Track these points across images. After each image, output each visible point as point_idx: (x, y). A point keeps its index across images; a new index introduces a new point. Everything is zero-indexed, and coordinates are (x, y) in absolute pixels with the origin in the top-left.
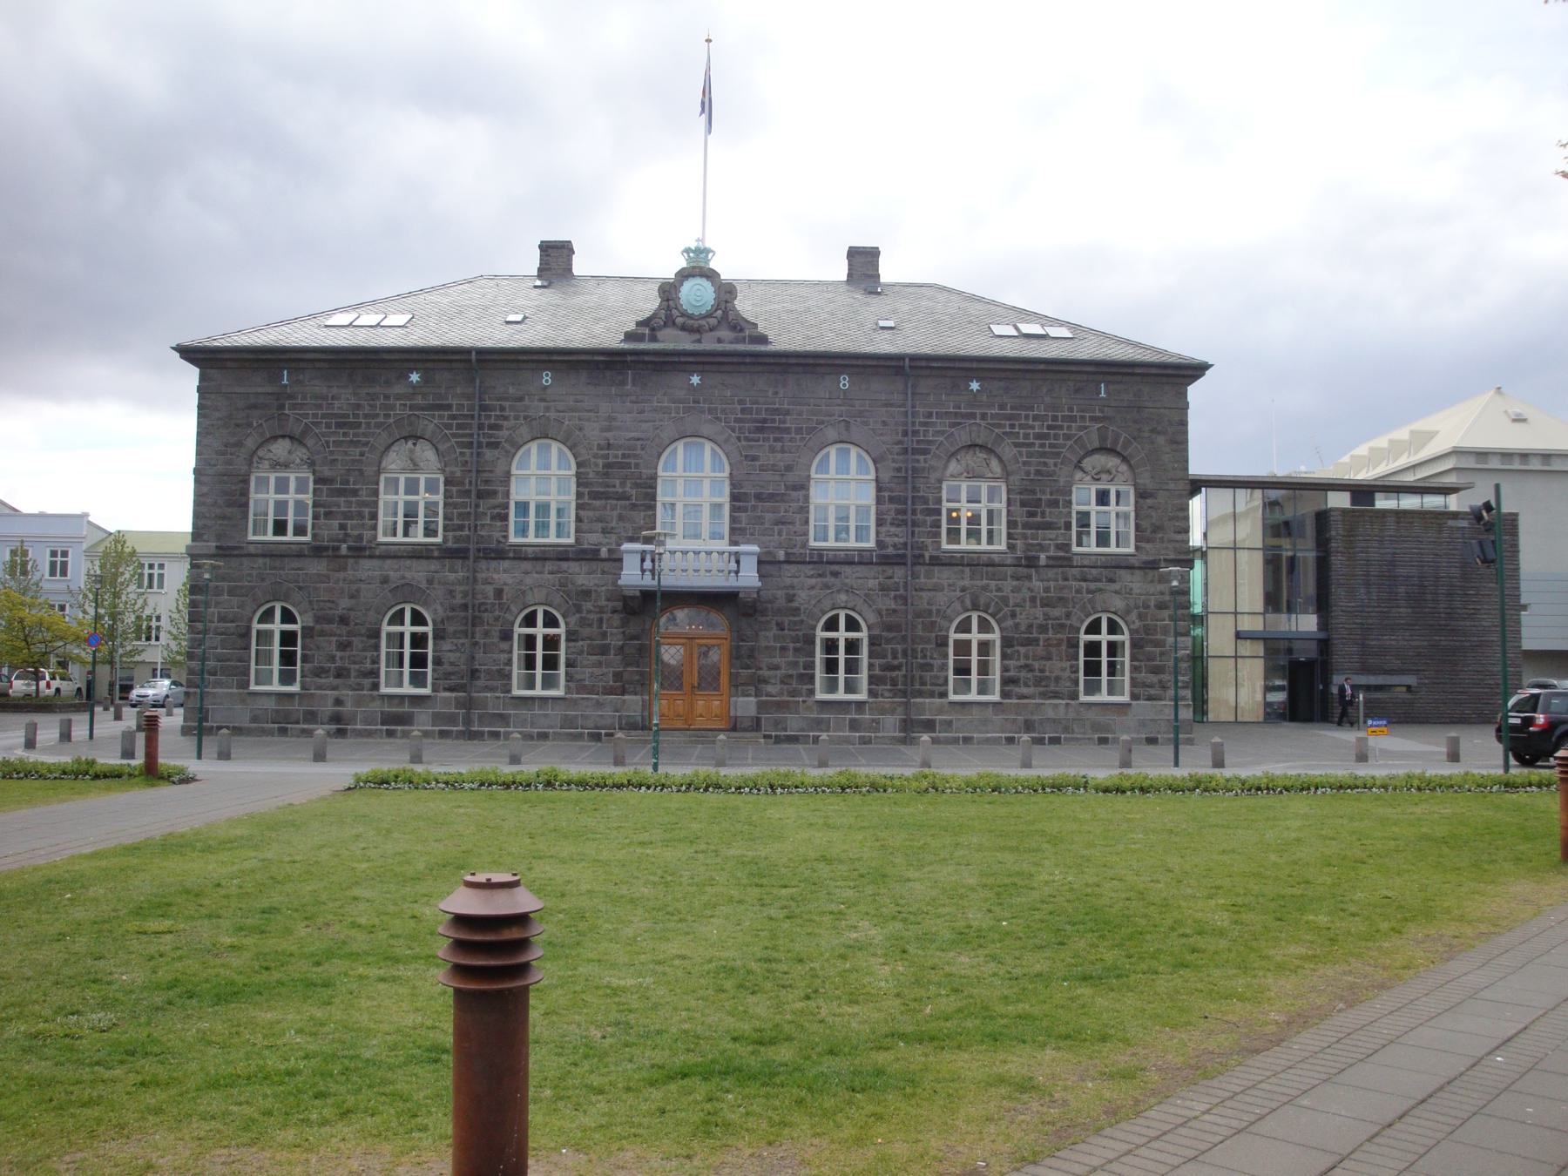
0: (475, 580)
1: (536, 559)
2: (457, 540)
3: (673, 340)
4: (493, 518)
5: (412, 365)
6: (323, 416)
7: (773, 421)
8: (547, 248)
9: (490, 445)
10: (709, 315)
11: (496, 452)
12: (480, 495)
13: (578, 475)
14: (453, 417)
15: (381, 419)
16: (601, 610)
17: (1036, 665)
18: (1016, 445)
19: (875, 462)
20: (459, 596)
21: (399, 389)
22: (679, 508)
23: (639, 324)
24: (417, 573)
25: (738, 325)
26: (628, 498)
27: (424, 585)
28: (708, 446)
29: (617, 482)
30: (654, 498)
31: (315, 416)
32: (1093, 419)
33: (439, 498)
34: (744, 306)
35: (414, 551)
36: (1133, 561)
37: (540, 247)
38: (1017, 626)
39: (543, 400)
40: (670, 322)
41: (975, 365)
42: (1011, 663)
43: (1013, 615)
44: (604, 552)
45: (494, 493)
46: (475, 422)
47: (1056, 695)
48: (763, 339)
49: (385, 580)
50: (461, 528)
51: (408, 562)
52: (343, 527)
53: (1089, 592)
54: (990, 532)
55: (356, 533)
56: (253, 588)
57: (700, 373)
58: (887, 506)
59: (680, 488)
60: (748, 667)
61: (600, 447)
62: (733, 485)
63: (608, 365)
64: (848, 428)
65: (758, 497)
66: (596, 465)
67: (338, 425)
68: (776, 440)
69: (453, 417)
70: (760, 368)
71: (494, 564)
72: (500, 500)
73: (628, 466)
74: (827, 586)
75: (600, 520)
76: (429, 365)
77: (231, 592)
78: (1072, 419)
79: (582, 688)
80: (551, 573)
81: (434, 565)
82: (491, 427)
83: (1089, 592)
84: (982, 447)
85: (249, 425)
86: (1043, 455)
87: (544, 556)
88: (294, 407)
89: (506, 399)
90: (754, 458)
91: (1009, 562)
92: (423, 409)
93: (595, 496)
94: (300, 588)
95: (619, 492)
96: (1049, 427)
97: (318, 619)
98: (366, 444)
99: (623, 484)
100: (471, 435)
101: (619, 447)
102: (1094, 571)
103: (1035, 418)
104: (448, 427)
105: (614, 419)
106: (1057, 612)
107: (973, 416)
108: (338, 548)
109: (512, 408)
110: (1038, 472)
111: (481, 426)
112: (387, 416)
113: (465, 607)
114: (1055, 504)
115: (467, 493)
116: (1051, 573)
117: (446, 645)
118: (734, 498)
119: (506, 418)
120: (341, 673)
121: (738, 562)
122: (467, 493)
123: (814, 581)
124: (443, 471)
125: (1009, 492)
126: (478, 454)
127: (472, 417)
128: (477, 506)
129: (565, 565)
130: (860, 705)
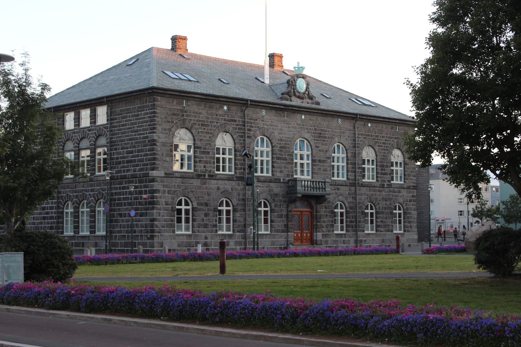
1: (262, 182)
3: (296, 102)
5: (225, 103)
8: (175, 39)
10: (304, 93)
11: (250, 140)
13: (272, 151)
14: (237, 125)
15: (215, 124)
17: (384, 220)
18: (379, 146)
19: (346, 150)
20: (241, 195)
21: (220, 112)
24: (228, 185)
25: (311, 98)
26: (287, 160)
27: (230, 191)
31: (194, 120)
32: (396, 138)
34: (313, 92)
35: (228, 177)
36: (405, 186)
37: (171, 39)
38: (379, 207)
39: (263, 121)
42: (378, 220)
43: (379, 204)
44: (282, 180)
47: (388, 231)
48: (318, 103)
49: (218, 189)
51: (226, 182)
52: (205, 167)
53: (395, 196)
54: (338, 173)
55: (209, 169)
56: (176, 191)
57: (304, 114)
58: (350, 166)
60: (319, 222)
63: (282, 110)
64: (340, 138)
65: (320, 161)
67: (202, 125)
68: (324, 141)
69: (237, 125)
70: (319, 115)
76: (231, 104)
77: (169, 192)
78: (390, 138)
79: (277, 231)
81: (233, 183)
83: (395, 196)
84: (371, 146)
85: (172, 122)
86: (385, 150)
88: (187, 116)
89: (252, 119)
90: (318, 147)
91: (378, 186)
92: (227, 121)
93: (278, 158)
94: (192, 191)
96: (386, 140)
97: (198, 204)
98: (211, 133)
102: (396, 189)
103: (383, 137)
104: (236, 129)
106: (388, 203)
107: (368, 135)
108: (204, 176)
110: (383, 156)
112: (217, 122)
113: (244, 200)
114: (387, 166)
116: (386, 190)
117: (238, 214)
118: (313, 161)
119: (252, 127)
120: (206, 226)
125: (376, 162)
130: (345, 234)
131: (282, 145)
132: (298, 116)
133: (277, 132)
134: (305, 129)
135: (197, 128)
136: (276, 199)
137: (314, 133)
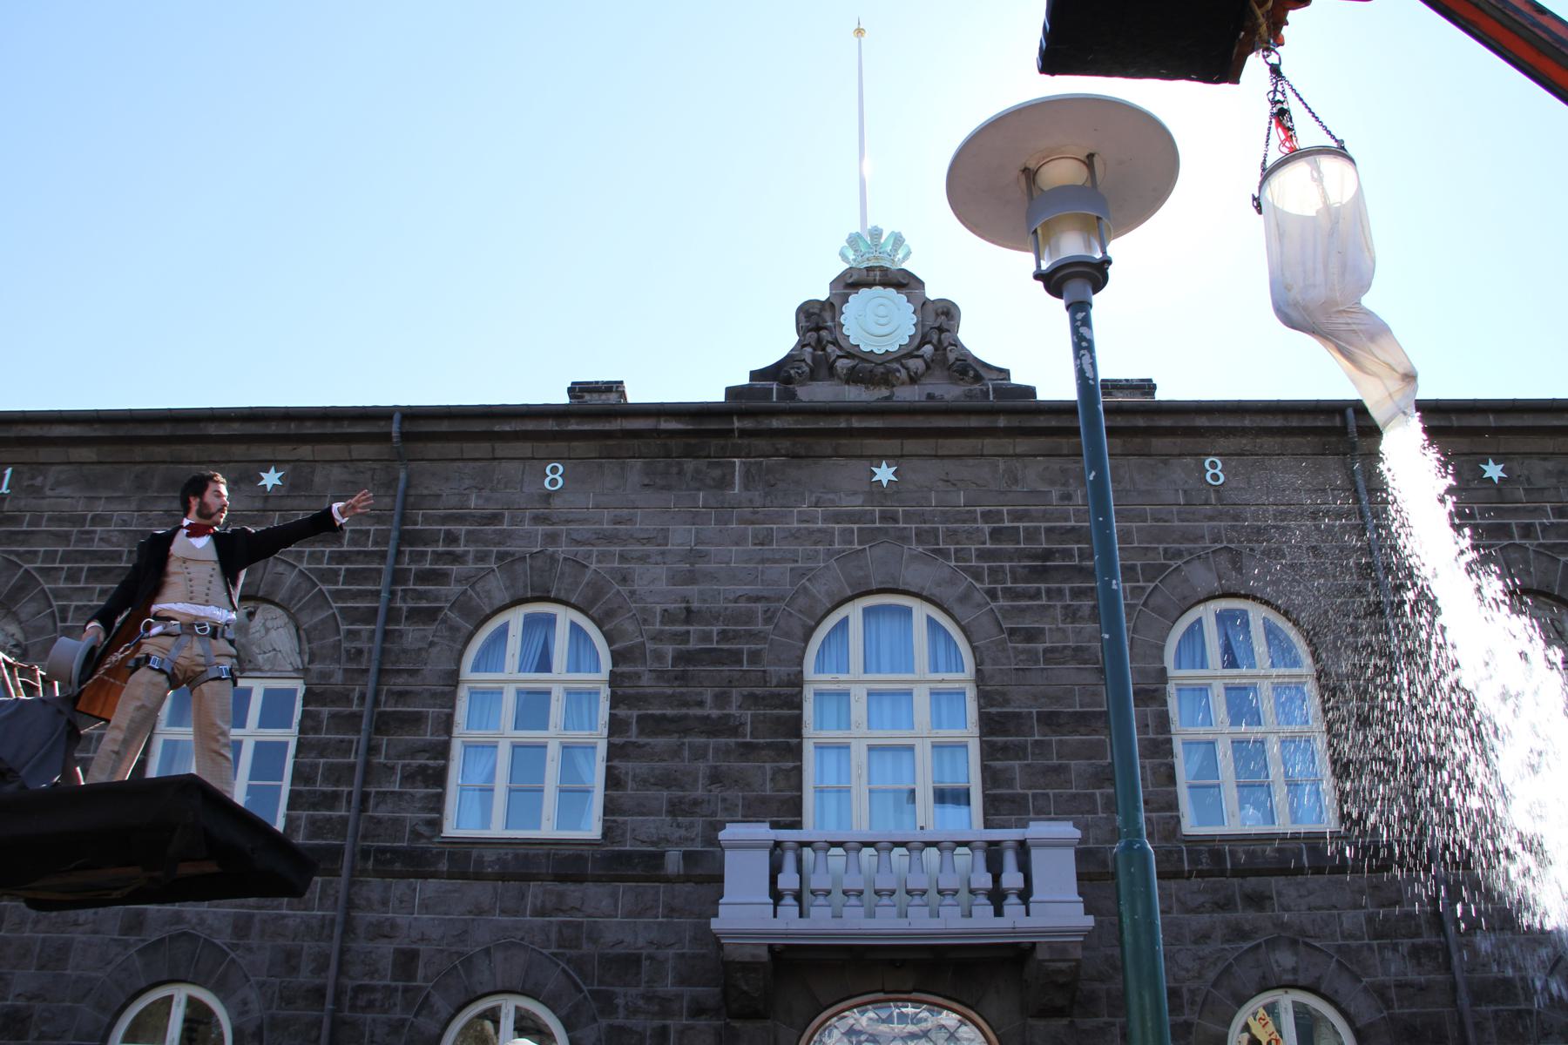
0: (349, 928)
1: (503, 877)
2: (316, 828)
4: (409, 778)
6: (67, 557)
7: (1067, 554)
9: (416, 615)
12: (383, 723)
13: (615, 680)
14: (342, 557)
16: (665, 1006)
22: (859, 752)
23: (755, 375)
26: (735, 731)
28: (921, 611)
29: (708, 694)
30: (795, 727)
31: (51, 556)
33: (289, 736)
40: (822, 369)
41: (1492, 421)
44: (673, 862)
45: (416, 720)
46: (386, 568)
50: (331, 800)
57: (891, 458)
59: (859, 708)
61: (667, 616)
62: (984, 697)
65: (1050, 720)
66: (659, 656)
68: (1077, 594)
69: (342, 557)
71: (399, 887)
72: (428, 736)
73: (735, 657)
74: (1238, 933)
75: (666, 781)
76: (305, 451)
80: (540, 912)
82: (424, 577)
87: (525, 864)
89: (460, 519)
90: (1032, 635)
95: (710, 720)
99: (722, 699)
100: (377, 593)
101: (715, 617)
105: (702, 556)
109: (472, 537)
111: (398, 577)
115: (353, 721)
118: (990, 724)
119: (457, 558)
121: (1024, 867)
122: (353, 721)
123: (1205, 918)
124: (303, 672)
126: (387, 635)
127: (382, 556)
128: (372, 749)
129: (573, 892)
131: (693, 645)
132: (843, 473)
133: (661, 571)
134: (903, 538)
135: (58, 594)
136: (625, 995)
137: (982, 555)
